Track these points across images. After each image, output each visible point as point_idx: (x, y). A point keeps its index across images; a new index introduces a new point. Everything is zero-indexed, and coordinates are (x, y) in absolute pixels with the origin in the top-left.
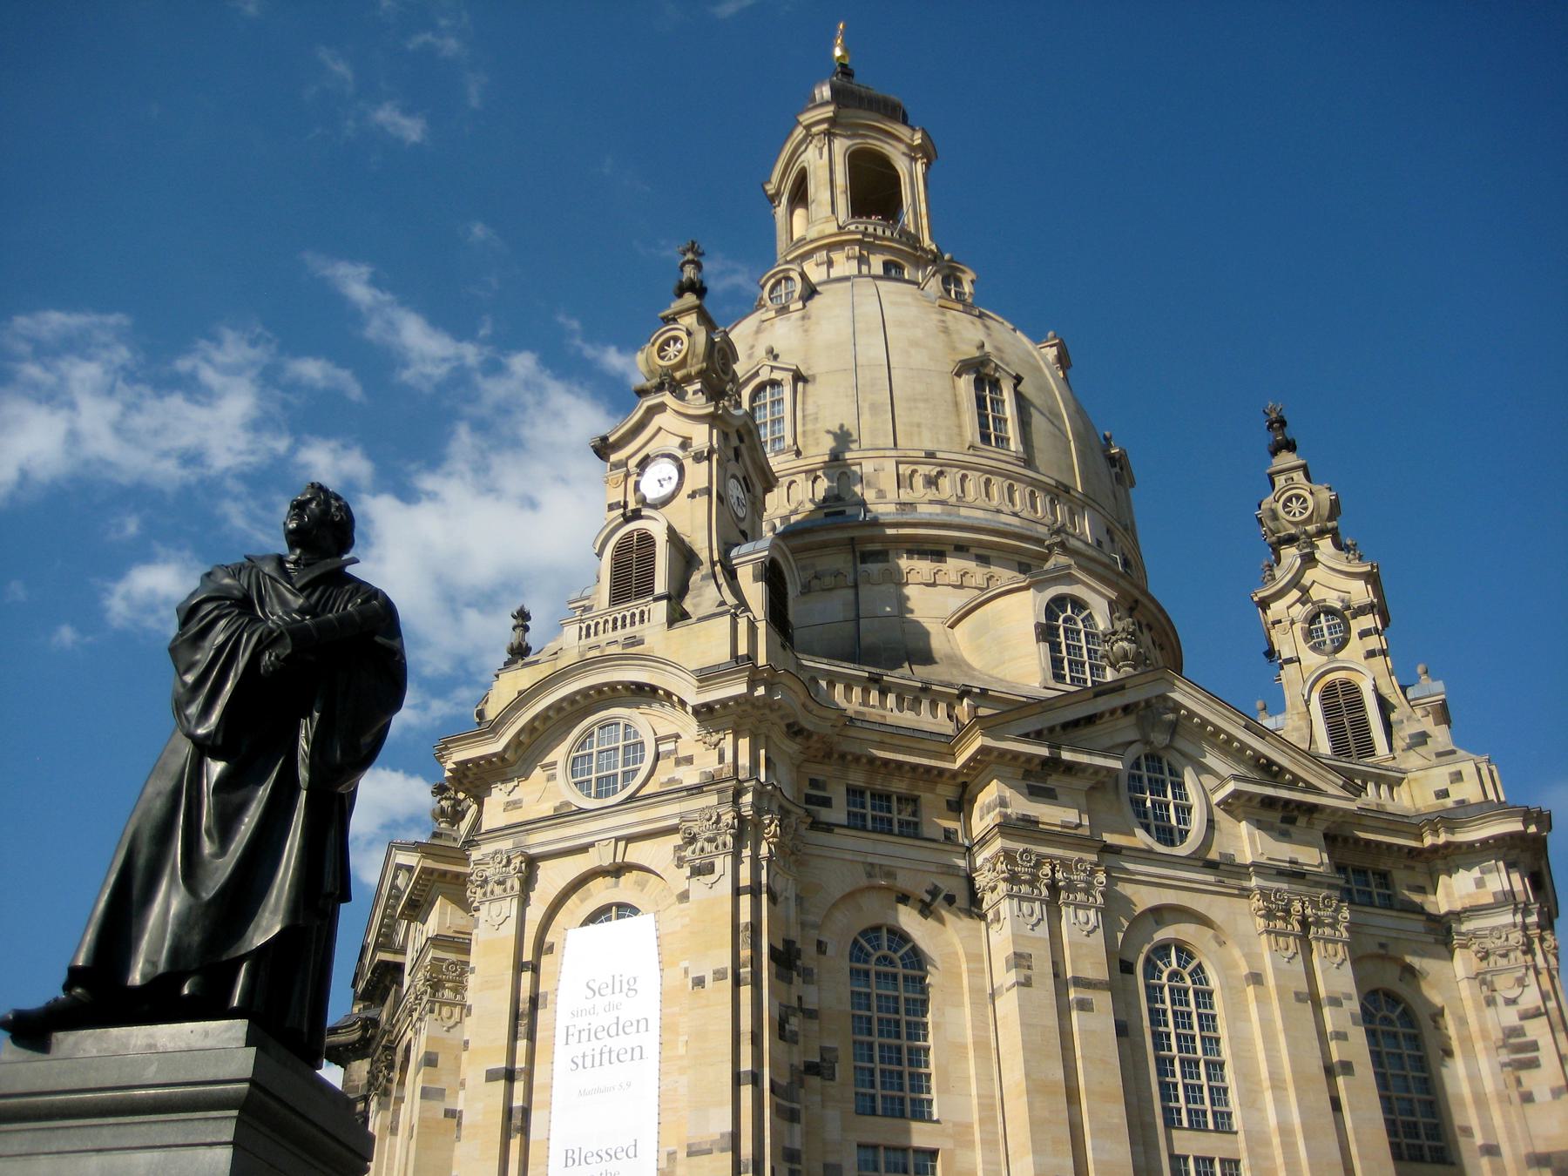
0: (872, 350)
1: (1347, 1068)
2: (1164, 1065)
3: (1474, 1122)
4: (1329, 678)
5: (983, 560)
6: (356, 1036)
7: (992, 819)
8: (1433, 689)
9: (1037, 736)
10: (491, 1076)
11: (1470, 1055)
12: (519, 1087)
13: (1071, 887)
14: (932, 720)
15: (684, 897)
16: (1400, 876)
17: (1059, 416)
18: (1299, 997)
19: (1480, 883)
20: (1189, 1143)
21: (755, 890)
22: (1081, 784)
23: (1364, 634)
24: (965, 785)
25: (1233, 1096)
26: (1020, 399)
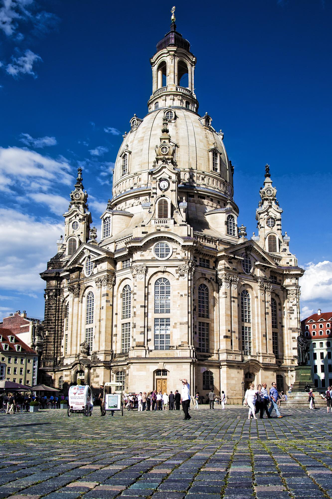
0: (192, 142)
1: (268, 313)
4: (271, 234)
6: (53, 275)
7: (222, 267)
9: (231, 253)
10: (141, 306)
12: (146, 309)
14: (212, 245)
15: (178, 279)
18: (263, 301)
19: (291, 281)
21: (191, 280)
22: (236, 261)
23: (278, 225)
24: (217, 259)
25: (251, 317)
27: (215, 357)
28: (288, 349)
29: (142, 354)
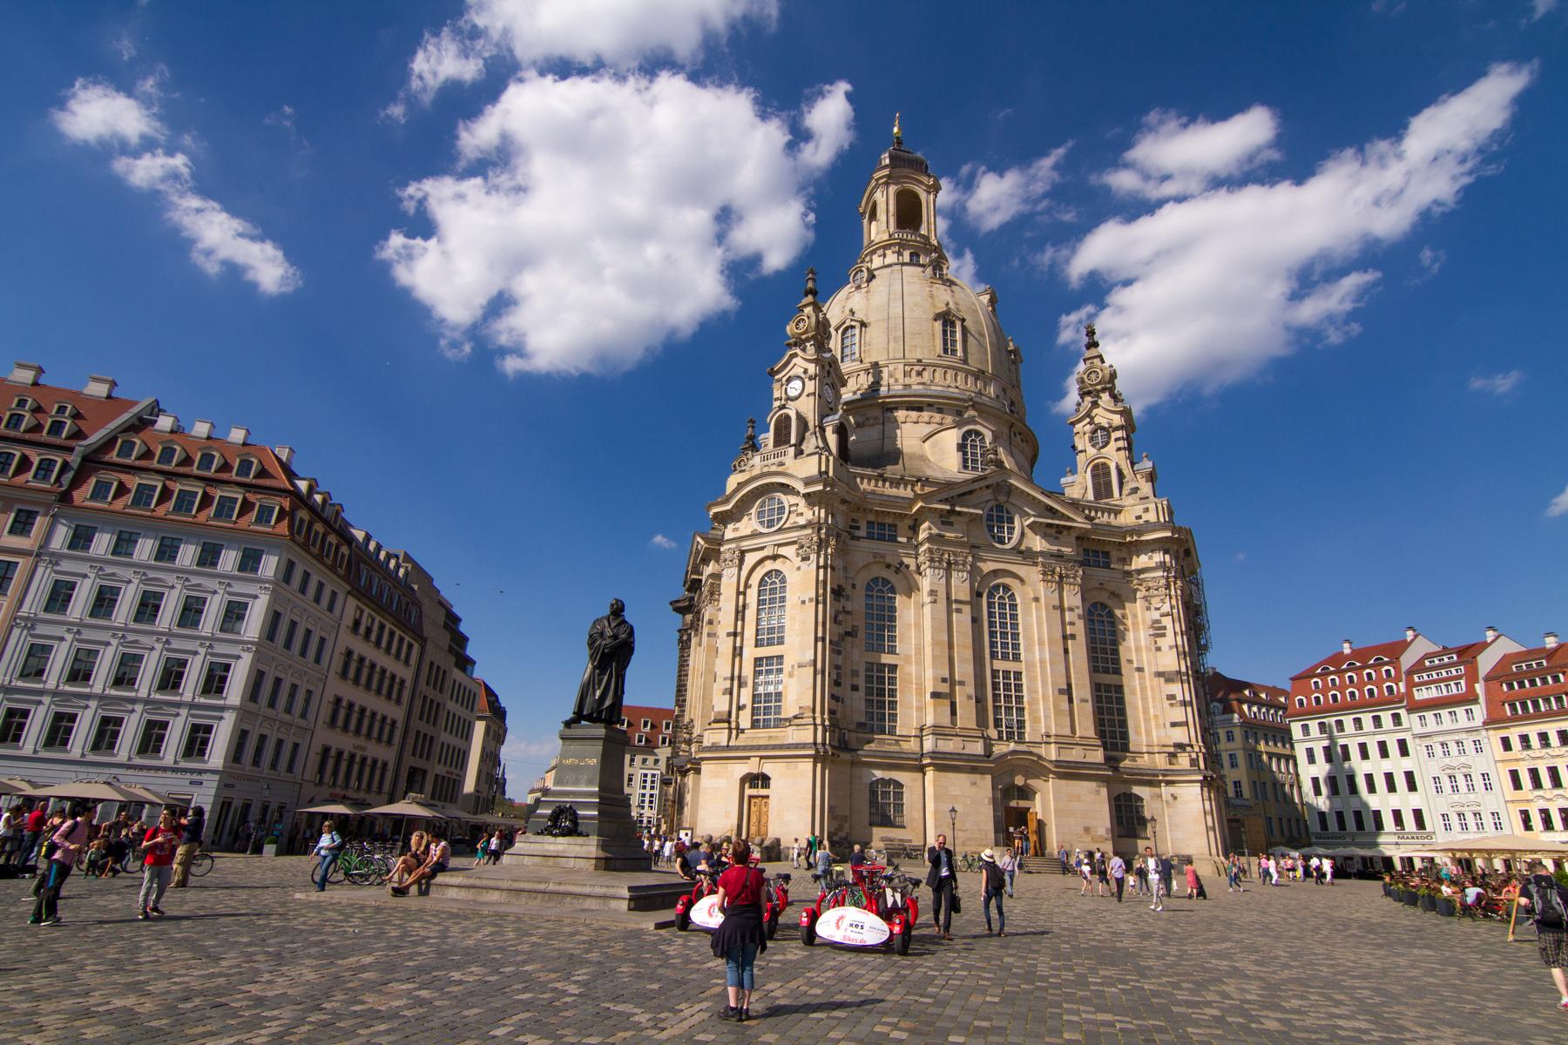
1: (1073, 637)
2: (992, 634)
3: (1134, 658)
5: (940, 411)
8: (1147, 465)
9: (945, 501)
10: (729, 635)
11: (1136, 630)
13: (956, 563)
14: (905, 492)
16: (1114, 554)
17: (983, 335)
20: (1000, 665)
21: (825, 567)
23: (1117, 440)
26: (964, 329)
27: (912, 746)
28: (1157, 726)
29: (721, 737)
